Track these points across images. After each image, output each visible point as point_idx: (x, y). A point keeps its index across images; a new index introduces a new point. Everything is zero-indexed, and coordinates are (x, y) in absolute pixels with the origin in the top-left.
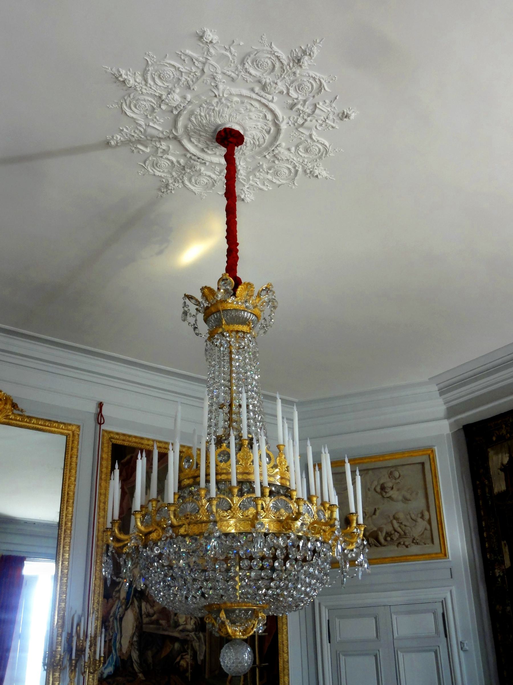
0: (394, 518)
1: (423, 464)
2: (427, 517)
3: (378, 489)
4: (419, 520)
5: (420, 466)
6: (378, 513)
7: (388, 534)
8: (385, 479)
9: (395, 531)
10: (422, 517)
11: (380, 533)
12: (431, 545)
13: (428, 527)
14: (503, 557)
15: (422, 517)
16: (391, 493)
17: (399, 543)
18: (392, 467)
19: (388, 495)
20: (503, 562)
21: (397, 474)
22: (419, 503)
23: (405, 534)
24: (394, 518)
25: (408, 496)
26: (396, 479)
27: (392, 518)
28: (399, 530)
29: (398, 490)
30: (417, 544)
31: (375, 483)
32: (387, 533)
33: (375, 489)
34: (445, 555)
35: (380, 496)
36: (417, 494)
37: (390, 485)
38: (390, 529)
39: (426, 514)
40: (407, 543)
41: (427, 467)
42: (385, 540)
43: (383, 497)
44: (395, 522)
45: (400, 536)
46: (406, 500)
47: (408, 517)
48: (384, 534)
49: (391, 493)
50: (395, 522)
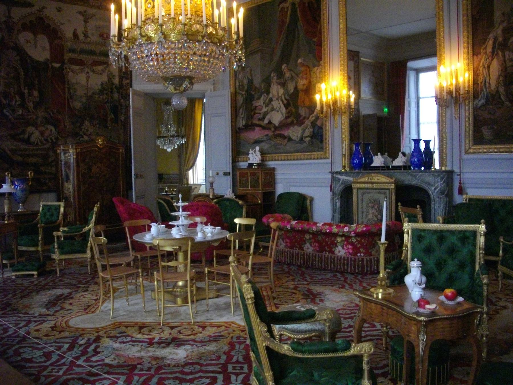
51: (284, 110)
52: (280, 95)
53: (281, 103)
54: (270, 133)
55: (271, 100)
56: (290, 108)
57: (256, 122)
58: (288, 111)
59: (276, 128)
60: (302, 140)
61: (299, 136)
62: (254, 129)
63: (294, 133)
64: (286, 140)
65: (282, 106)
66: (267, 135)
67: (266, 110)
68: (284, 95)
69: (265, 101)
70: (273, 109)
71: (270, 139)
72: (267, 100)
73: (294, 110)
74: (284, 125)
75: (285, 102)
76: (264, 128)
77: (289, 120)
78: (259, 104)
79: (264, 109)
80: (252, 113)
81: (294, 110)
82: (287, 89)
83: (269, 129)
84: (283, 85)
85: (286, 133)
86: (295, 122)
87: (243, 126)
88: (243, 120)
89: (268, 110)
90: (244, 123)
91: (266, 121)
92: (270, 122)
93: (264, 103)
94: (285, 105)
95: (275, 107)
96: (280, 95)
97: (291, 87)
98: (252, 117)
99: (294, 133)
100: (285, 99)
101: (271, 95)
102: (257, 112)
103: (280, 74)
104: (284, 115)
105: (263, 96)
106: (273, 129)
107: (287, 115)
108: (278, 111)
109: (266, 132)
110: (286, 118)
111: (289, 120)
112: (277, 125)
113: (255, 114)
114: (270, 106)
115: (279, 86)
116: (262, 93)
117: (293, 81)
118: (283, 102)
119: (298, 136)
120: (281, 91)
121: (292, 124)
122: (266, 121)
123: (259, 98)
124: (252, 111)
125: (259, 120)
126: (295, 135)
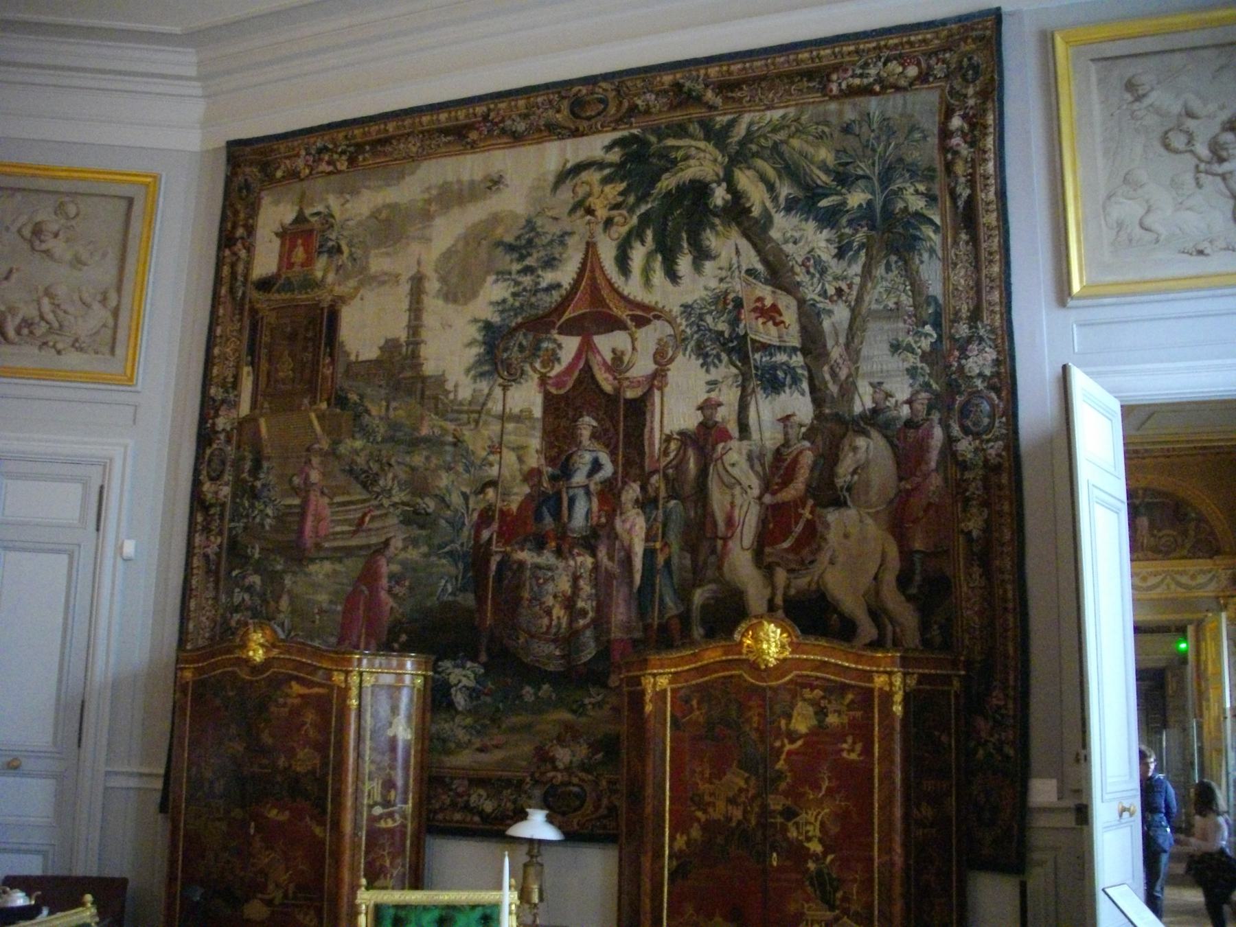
0: (47, 293)
1: (130, 201)
2: (113, 302)
3: (27, 232)
4: (96, 306)
5: (124, 204)
6: (15, 276)
7: (27, 323)
8: (45, 214)
9: (42, 318)
10: (104, 301)
11: (9, 318)
12: (108, 356)
13: (111, 322)
14: (238, 396)
15: (104, 301)
16: (50, 244)
17: (45, 344)
18: (68, 194)
19: (44, 247)
20: (235, 405)
21: (72, 210)
22: (101, 273)
23: (61, 326)
24: (47, 293)
25: (84, 256)
26: (68, 218)
27: (41, 293)
28: (50, 317)
29: (68, 240)
30: (81, 349)
31: (23, 219)
32: (24, 320)
33: (19, 231)
34: (131, 379)
35: (26, 246)
36: (104, 255)
37: (55, 227)
38: (30, 311)
39: (113, 296)
40: (60, 346)
41: (137, 208)
42: (18, 332)
43: (33, 249)
44: (46, 301)
45: (51, 330)
46: (78, 262)
47: (76, 297)
48: (18, 320)
49: (50, 244)
50: (46, 301)
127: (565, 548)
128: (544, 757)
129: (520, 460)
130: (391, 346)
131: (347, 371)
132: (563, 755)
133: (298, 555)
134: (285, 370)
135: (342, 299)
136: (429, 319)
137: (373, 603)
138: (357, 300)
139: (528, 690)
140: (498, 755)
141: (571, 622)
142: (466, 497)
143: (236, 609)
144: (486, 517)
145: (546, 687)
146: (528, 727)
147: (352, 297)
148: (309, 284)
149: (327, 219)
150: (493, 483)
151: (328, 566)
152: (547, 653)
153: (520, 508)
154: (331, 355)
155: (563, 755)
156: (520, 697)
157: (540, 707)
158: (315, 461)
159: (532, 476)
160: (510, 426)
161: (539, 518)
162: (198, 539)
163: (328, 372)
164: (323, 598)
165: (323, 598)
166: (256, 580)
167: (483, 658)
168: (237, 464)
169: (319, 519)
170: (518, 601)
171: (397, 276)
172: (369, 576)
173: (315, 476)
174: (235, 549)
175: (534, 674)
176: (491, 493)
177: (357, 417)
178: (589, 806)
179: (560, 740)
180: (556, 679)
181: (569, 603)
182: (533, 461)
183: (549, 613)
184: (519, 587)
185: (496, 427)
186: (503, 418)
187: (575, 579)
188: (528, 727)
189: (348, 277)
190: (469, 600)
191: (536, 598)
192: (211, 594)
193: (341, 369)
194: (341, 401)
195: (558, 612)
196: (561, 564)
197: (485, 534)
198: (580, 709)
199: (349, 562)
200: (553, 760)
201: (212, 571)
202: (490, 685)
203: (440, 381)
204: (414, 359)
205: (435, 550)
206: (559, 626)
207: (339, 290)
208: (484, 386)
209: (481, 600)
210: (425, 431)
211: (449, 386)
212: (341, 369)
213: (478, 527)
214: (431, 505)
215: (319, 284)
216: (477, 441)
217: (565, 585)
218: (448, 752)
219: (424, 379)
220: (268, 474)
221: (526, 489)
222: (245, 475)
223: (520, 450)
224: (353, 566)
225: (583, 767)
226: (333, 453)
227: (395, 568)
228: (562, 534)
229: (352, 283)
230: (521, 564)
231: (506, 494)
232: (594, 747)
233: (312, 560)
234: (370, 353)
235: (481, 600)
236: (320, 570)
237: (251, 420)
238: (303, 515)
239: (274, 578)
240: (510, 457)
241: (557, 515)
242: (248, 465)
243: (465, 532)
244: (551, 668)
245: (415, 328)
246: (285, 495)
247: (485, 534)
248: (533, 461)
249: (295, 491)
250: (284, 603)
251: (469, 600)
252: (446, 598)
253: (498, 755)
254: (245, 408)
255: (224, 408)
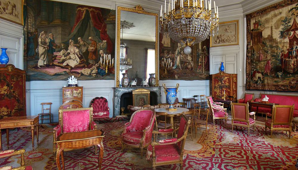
51: (79, 60)
52: (76, 52)
53: (77, 56)
54: (67, 71)
55: (69, 54)
56: (82, 59)
57: (55, 63)
58: (81, 60)
59: (72, 68)
60: (90, 75)
61: (89, 73)
62: (54, 68)
63: (85, 72)
64: (80, 75)
65: (77, 58)
66: (65, 72)
67: (65, 58)
68: (79, 53)
69: (65, 53)
70: (70, 58)
71: (68, 74)
72: (66, 53)
73: (85, 61)
74: (77, 67)
75: (80, 56)
76: (62, 67)
77: (82, 65)
78: (59, 54)
79: (63, 58)
80: (53, 59)
81: (85, 61)
82: (81, 50)
83: (67, 68)
84: (78, 47)
85: (79, 71)
86: (86, 66)
87: (45, 65)
88: (44, 62)
89: (66, 59)
90: (45, 63)
91: (65, 64)
92: (68, 65)
93: (63, 55)
94: (79, 58)
95: (72, 57)
96: (76, 52)
97: (84, 49)
98: (53, 61)
99: (85, 72)
100: (79, 54)
101: (69, 51)
102: (57, 58)
103: (76, 42)
104: (79, 63)
105: (62, 51)
106: (70, 69)
107: (80, 63)
108: (74, 60)
109: (65, 70)
110: (80, 64)
111: (82, 65)
112: (73, 66)
113: (55, 59)
114: (68, 57)
115: (75, 48)
116: (63, 49)
117: (85, 46)
118: (78, 56)
119: (88, 73)
120: (77, 50)
121: (84, 67)
122: (65, 64)
123: (59, 51)
124: (53, 57)
125: (59, 63)
126: (86, 72)
127: (293, 58)
128: (290, 83)
129: (286, 48)
130: (269, 36)
131: (264, 39)
132: (293, 83)
133: (259, 61)
134: (256, 40)
135: (262, 31)
136: (273, 32)
137: (269, 66)
138: (264, 31)
139: (288, 75)
140: (285, 83)
141: (294, 67)
142: (279, 53)
143: (252, 68)
144: (282, 55)
145: (290, 75)
146: (289, 79)
147: (263, 30)
148: (258, 29)
149: (259, 21)
150: (283, 51)
151: (263, 62)
152: (292, 71)
153: (287, 53)
154: (262, 38)
155: (293, 83)
156: (287, 76)
157: (290, 77)
158: (261, 50)
159: (288, 50)
160: (285, 44)
161: (289, 55)
162: (247, 60)
163: (261, 40)
164: (263, 66)
165: (263, 66)
166: (255, 64)
167: (283, 72)
168: (251, 52)
169: (262, 57)
170: (287, 65)
171: (269, 27)
172: (268, 63)
173: (261, 52)
174: (252, 61)
175: (289, 73)
176: (283, 52)
177: (265, 45)
178: (296, 88)
179: (292, 81)
180: (291, 74)
181: (293, 65)
182: (288, 48)
183: (291, 66)
184: (287, 63)
185: (283, 44)
186: (284, 43)
187: (294, 62)
188: (289, 79)
189: (263, 28)
190: (280, 65)
191: (289, 64)
192: (249, 66)
193: (263, 39)
194: (263, 43)
195: (292, 66)
196: (292, 60)
197: (282, 57)
198: (295, 77)
199: (265, 61)
200: (291, 83)
201: (249, 64)
202: (284, 75)
203: (275, 39)
204: (272, 37)
205: (276, 59)
206: (292, 67)
207: (262, 30)
208: (281, 39)
209: (282, 65)
210: (274, 46)
211: (277, 40)
212: (263, 39)
213: (281, 56)
214: (275, 54)
215: (259, 29)
216: (280, 46)
217: (293, 62)
218: (279, 83)
219: (273, 39)
220: (255, 52)
221: (287, 51)
222: (252, 53)
223: (286, 47)
224: (266, 62)
225: (295, 84)
226: (263, 49)
227: (271, 62)
228: (292, 57)
229: (263, 28)
230: (287, 60)
231: (285, 52)
232: (297, 81)
233: (261, 62)
234: (266, 37)
235: (282, 65)
236: (262, 63)
237: (252, 46)
238: (260, 57)
239: (257, 64)
240: (285, 48)
241: (291, 54)
242: (252, 51)
243: (280, 57)
244: (291, 72)
245: (272, 33)
246: (257, 54)
247: (282, 57)
248: (288, 48)
249: (259, 54)
250: (258, 67)
251: (280, 65)
252: (278, 65)
253: (285, 83)
254: (251, 45)
255: (249, 45)
